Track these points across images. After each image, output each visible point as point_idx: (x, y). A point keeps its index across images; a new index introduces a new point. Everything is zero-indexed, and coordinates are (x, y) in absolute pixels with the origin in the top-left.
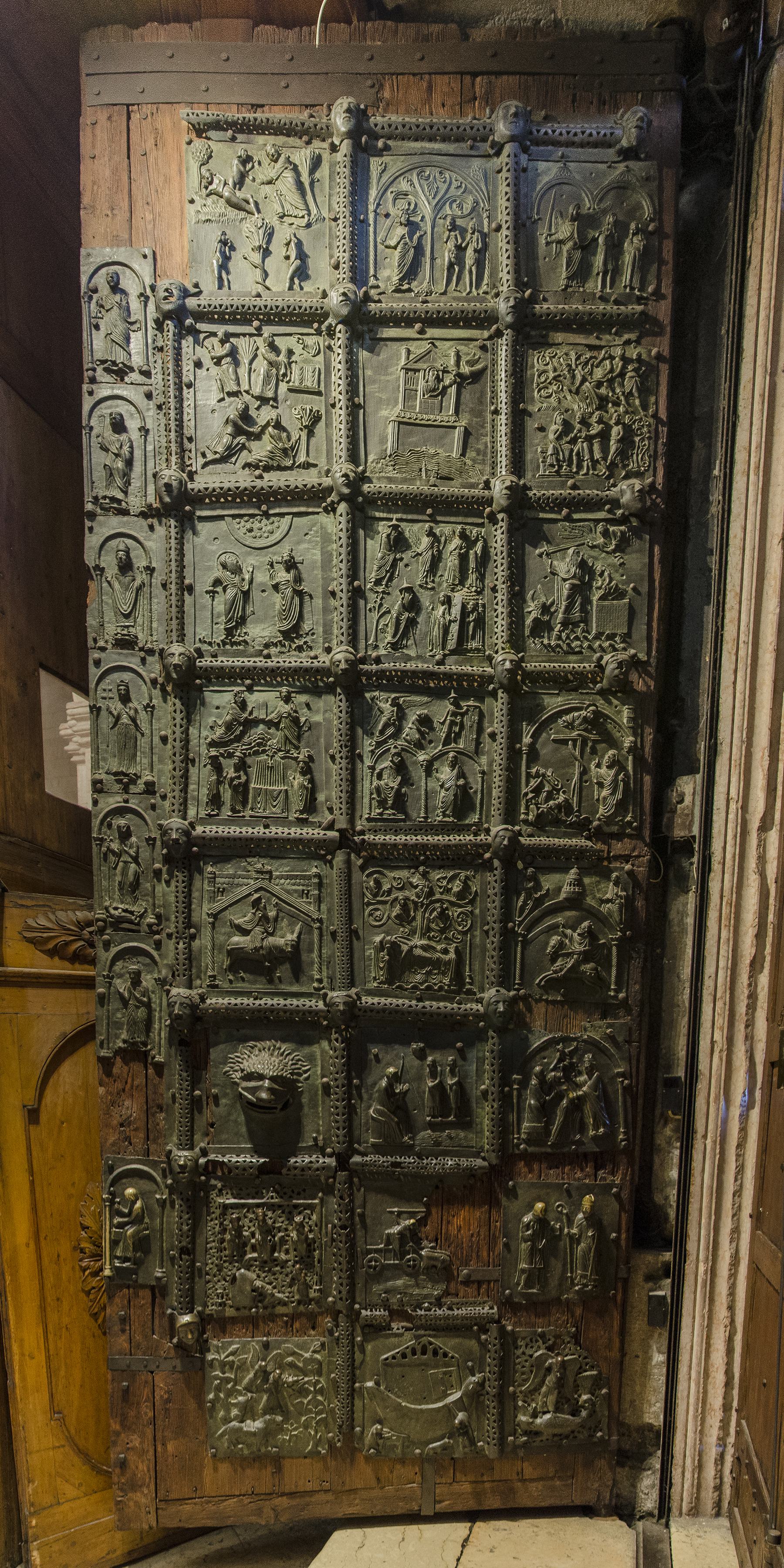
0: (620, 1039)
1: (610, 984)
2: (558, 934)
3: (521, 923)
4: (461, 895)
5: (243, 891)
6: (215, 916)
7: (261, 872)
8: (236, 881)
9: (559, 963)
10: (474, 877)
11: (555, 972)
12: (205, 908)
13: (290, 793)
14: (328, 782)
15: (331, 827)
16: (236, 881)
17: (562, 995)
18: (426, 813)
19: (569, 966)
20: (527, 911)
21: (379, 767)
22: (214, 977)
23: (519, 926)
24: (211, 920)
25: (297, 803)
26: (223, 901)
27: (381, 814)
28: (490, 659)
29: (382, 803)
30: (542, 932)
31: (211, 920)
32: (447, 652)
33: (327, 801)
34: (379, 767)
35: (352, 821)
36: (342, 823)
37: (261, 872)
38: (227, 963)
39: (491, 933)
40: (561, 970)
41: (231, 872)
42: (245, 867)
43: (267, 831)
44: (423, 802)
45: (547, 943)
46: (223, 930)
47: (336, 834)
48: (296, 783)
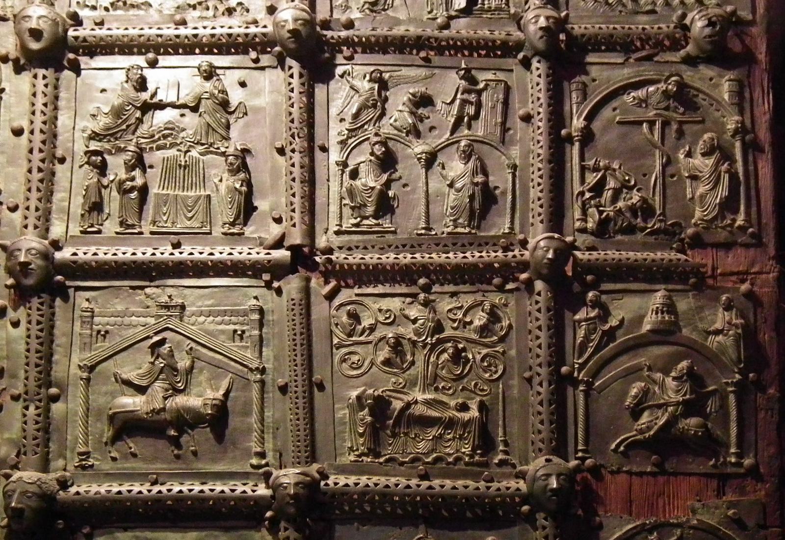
0: (751, 523)
1: (728, 447)
2: (640, 379)
3: (582, 366)
4: (484, 330)
5: (139, 332)
6: (91, 369)
7: (167, 307)
8: (127, 320)
9: (645, 418)
10: (506, 305)
11: (641, 432)
12: (75, 359)
13: (214, 200)
14: (274, 185)
15: (278, 244)
16: (127, 320)
17: (654, 465)
18: (428, 222)
19: (661, 422)
20: (590, 350)
21: (352, 164)
22: (87, 454)
23: (580, 370)
24: (85, 375)
25: (224, 213)
26: (103, 347)
27: (357, 225)
28: (517, 20)
29: (358, 208)
30: (614, 379)
31: (85, 375)
32: (453, 13)
33: (272, 210)
34: (352, 164)
35: (311, 233)
36: (296, 238)
37: (167, 307)
38: (108, 434)
39: (537, 380)
40: (649, 428)
41: (120, 308)
42: (141, 302)
43: (176, 252)
44: (422, 208)
45: (625, 393)
46: (104, 389)
47: (288, 253)
48: (223, 187)
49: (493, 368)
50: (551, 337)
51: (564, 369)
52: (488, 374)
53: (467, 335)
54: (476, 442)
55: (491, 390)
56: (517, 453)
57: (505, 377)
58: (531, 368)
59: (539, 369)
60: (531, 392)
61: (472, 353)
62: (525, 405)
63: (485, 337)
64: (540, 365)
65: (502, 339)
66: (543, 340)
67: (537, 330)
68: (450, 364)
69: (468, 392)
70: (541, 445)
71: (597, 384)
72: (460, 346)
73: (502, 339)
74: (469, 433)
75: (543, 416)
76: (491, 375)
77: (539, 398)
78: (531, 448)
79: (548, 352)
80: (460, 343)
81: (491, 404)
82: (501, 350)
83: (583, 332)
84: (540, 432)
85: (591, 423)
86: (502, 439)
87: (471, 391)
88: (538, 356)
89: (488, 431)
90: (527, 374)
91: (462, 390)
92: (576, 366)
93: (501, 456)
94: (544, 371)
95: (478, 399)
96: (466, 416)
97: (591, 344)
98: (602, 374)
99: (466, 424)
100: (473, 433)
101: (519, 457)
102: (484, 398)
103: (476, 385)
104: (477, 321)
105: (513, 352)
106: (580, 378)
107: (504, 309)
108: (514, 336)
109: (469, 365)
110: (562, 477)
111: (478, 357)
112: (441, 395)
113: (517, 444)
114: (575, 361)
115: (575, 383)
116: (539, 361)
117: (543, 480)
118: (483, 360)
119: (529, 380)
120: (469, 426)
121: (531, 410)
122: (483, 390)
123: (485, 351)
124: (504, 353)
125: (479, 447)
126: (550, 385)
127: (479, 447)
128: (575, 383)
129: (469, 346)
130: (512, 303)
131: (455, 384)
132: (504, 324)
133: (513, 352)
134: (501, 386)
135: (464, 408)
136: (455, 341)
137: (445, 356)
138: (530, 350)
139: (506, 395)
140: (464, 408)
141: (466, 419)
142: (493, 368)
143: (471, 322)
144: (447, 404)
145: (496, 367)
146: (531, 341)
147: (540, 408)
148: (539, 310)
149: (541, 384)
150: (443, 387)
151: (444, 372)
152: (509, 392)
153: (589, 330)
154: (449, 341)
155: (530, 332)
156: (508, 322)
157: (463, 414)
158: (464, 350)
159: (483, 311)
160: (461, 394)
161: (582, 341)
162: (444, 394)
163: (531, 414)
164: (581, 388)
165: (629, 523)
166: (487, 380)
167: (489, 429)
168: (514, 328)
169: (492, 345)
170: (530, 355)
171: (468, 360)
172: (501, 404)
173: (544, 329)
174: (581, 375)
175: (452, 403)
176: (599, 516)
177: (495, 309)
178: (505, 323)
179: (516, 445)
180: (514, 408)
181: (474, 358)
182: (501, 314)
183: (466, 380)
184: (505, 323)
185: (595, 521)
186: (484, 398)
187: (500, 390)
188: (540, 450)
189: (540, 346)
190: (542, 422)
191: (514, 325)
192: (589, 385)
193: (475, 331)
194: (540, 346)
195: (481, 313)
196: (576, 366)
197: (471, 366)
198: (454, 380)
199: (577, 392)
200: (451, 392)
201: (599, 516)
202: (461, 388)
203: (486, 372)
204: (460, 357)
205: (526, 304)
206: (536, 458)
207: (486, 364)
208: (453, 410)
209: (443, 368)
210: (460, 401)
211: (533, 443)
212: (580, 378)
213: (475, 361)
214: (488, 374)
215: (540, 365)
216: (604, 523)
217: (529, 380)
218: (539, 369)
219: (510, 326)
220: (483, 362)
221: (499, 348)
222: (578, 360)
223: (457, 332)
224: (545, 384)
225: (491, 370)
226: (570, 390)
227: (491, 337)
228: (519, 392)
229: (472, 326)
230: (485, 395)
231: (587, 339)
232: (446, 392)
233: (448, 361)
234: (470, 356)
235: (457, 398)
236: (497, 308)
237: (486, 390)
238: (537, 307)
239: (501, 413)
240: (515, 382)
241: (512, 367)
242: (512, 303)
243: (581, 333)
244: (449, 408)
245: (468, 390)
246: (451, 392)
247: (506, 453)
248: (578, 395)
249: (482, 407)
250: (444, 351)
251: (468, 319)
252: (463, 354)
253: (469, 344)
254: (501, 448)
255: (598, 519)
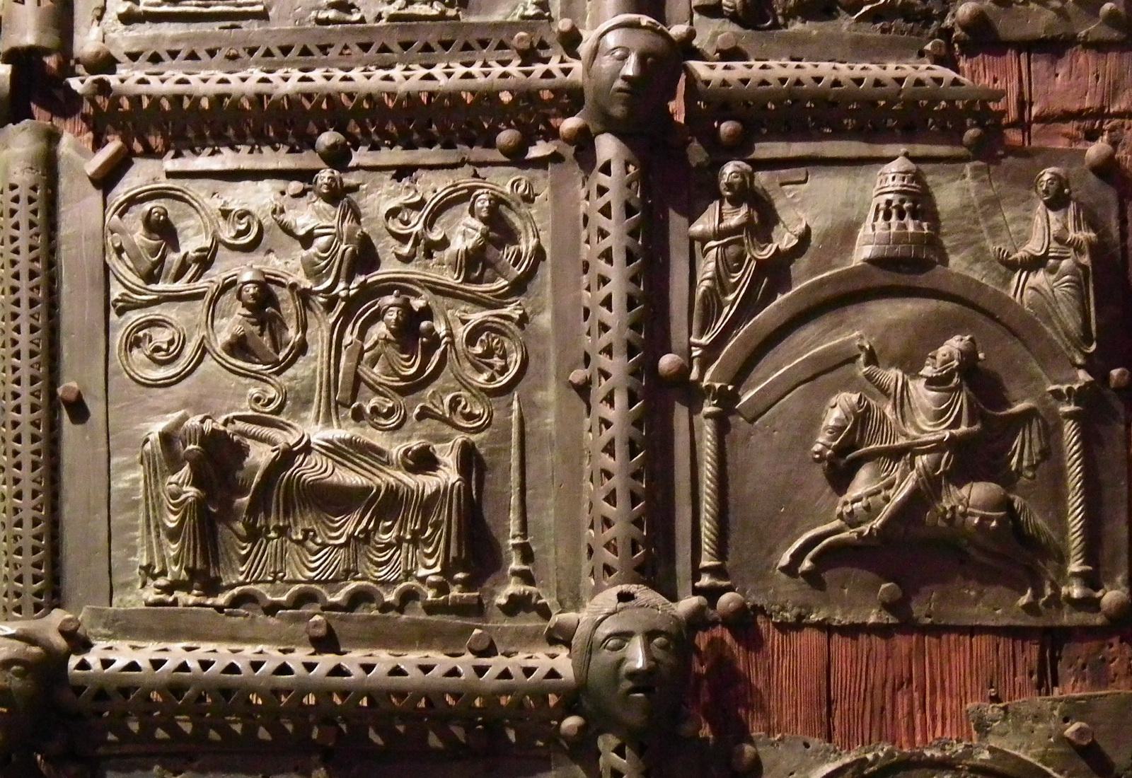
3: (711, 352)
10: (528, 199)
20: (728, 312)
23: (705, 365)
39: (600, 389)
49: (497, 362)
50: (634, 279)
51: (666, 362)
52: (485, 376)
53: (433, 275)
54: (453, 552)
55: (490, 415)
56: (552, 578)
57: (523, 384)
58: (587, 360)
59: (604, 361)
60: (588, 421)
61: (447, 321)
62: (573, 454)
63: (479, 281)
64: (608, 351)
65: (519, 287)
66: (617, 288)
67: (602, 262)
68: (390, 350)
69: (436, 422)
70: (609, 557)
71: (745, 399)
72: (417, 304)
73: (519, 287)
74: (436, 526)
75: (615, 482)
76: (492, 379)
77: (607, 434)
78: (586, 565)
79: (627, 317)
80: (417, 295)
81: (492, 452)
82: (516, 315)
83: (712, 265)
84: (607, 522)
85: (732, 501)
86: (517, 541)
87: (442, 419)
88: (604, 328)
89: (482, 521)
90: (578, 375)
91: (420, 417)
92: (696, 352)
93: (514, 587)
94: (617, 365)
95: (459, 438)
96: (428, 483)
97: (731, 297)
98: (755, 375)
99: (428, 505)
100: (444, 527)
101: (559, 590)
102: (474, 438)
103: (455, 402)
104: (460, 238)
105: (545, 320)
106: (705, 383)
107: (524, 209)
108: (549, 276)
109: (438, 352)
110: (657, 641)
111: (461, 332)
112: (369, 430)
113: (551, 555)
114: (693, 339)
115: (693, 395)
116: (605, 339)
117: (614, 649)
118: (472, 339)
119: (583, 389)
120: (436, 510)
121: (587, 467)
122: (470, 417)
123: (477, 316)
124: (523, 321)
125: (459, 564)
126: (631, 403)
127: (459, 564)
128: (693, 395)
129: (438, 303)
130: (544, 192)
131: (402, 401)
132: (523, 247)
133: (545, 320)
134: (515, 405)
135: (424, 461)
136: (404, 291)
137: (380, 330)
138: (587, 312)
139: (527, 429)
140: (424, 461)
141: (428, 491)
142: (497, 362)
143: (444, 243)
144: (381, 452)
145: (504, 357)
146: (588, 289)
147: (608, 462)
148: (606, 211)
149: (609, 399)
150: (374, 410)
151: (376, 370)
152: (535, 421)
153: (725, 259)
154: (388, 291)
155: (586, 267)
156: (533, 242)
157: (421, 478)
158: (427, 313)
159: (472, 212)
160: (418, 426)
161: (708, 287)
162: (376, 426)
163: (586, 477)
164: (708, 409)
165: (824, 760)
166: (482, 389)
167: (486, 515)
168: (548, 257)
169: (498, 300)
170: (586, 325)
171: (435, 341)
172: (514, 452)
173: (619, 257)
174: (708, 376)
175: (394, 451)
176: (751, 741)
177: (502, 208)
178: (527, 245)
179: (551, 557)
180: (545, 461)
181: (450, 334)
182: (518, 224)
183: (429, 391)
184: (527, 245)
185: (742, 752)
186: (474, 438)
187: (515, 416)
188: (608, 570)
189: (607, 302)
190: (611, 498)
191: (547, 250)
192: (727, 400)
193: (454, 265)
194: (607, 302)
195: (469, 220)
196: (696, 352)
197: (444, 353)
198: (402, 392)
199: (699, 418)
200: (393, 421)
201: (751, 741)
202: (417, 410)
203: (480, 371)
204: (418, 333)
205: (576, 194)
206: (597, 590)
207: (478, 349)
208: (398, 468)
209: (373, 363)
210: (415, 444)
211: (591, 552)
212: (705, 383)
213: (452, 343)
214: (485, 376)
215: (608, 351)
216: (766, 760)
217: (583, 389)
218: (604, 361)
219: (539, 253)
220: (474, 345)
221: (512, 310)
222: (702, 333)
223: (410, 268)
224: (620, 399)
225: (491, 366)
226: (681, 414)
227: (493, 281)
228: (560, 419)
229: (447, 252)
230: (478, 430)
231: (720, 280)
232: (383, 421)
233: (387, 341)
234: (441, 329)
235: (409, 438)
236: (508, 205)
237: (479, 417)
238: (601, 202)
239: (514, 476)
240: (549, 394)
241: (543, 358)
242: (544, 192)
243: (707, 268)
244: (388, 463)
245: (435, 416)
246: (393, 421)
247: (526, 578)
248: (702, 426)
249: (469, 459)
250: (377, 316)
251: (436, 235)
252: (424, 324)
253: (440, 298)
254: (515, 565)
255: (748, 748)
